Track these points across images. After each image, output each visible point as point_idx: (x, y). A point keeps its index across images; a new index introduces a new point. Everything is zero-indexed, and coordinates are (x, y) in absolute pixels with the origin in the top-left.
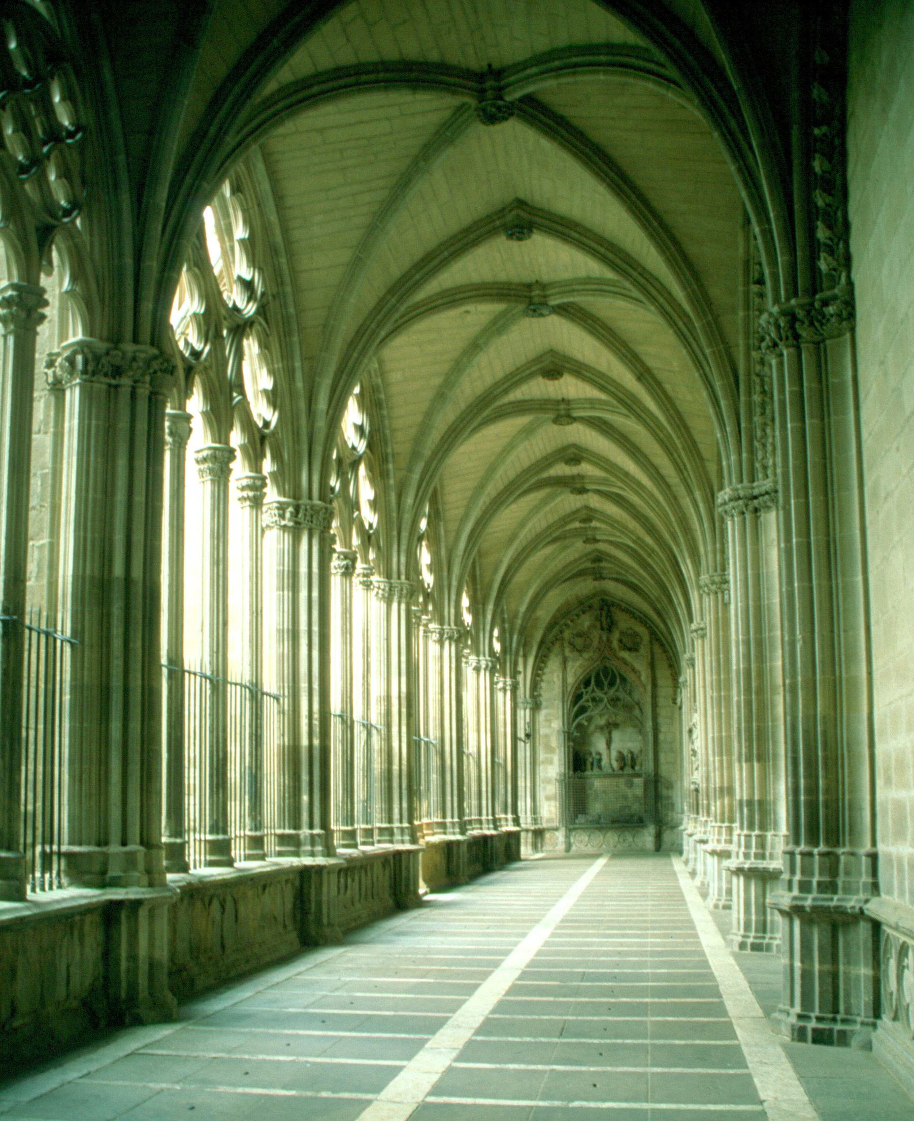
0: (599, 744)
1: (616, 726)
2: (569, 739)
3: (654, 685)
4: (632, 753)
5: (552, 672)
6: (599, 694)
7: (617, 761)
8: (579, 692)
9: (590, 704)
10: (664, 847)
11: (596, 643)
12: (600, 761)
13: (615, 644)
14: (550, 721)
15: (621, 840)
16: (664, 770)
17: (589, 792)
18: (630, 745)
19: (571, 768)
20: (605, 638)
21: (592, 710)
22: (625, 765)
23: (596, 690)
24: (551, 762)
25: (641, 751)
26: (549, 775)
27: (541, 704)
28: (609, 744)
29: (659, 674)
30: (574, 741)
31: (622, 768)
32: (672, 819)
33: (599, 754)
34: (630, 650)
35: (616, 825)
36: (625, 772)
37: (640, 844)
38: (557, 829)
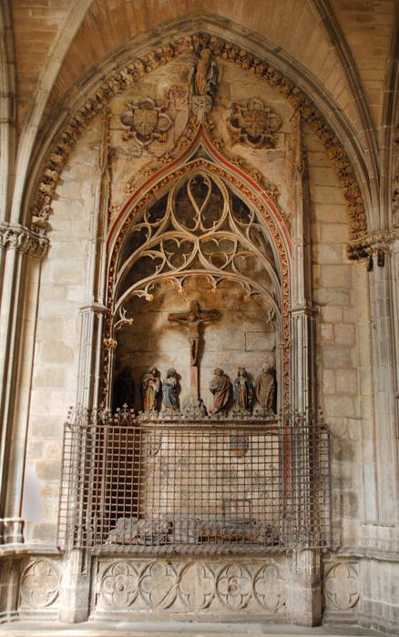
0: (174, 352)
1: (215, 316)
2: (106, 329)
3: (309, 219)
4: (246, 375)
5: (79, 180)
6: (182, 233)
7: (214, 392)
10: (332, 609)
11: (180, 126)
13: (223, 130)
15: (223, 588)
16: (332, 411)
18: (242, 359)
20: (200, 117)
21: (166, 269)
22: (231, 402)
23: (176, 223)
24: (60, 384)
25: (272, 372)
26: (54, 413)
27: (47, 245)
28: (197, 352)
29: (318, 195)
30: (117, 335)
31: (224, 408)
32: (353, 540)
34: (254, 140)
35: (209, 548)
38: (60, 555)
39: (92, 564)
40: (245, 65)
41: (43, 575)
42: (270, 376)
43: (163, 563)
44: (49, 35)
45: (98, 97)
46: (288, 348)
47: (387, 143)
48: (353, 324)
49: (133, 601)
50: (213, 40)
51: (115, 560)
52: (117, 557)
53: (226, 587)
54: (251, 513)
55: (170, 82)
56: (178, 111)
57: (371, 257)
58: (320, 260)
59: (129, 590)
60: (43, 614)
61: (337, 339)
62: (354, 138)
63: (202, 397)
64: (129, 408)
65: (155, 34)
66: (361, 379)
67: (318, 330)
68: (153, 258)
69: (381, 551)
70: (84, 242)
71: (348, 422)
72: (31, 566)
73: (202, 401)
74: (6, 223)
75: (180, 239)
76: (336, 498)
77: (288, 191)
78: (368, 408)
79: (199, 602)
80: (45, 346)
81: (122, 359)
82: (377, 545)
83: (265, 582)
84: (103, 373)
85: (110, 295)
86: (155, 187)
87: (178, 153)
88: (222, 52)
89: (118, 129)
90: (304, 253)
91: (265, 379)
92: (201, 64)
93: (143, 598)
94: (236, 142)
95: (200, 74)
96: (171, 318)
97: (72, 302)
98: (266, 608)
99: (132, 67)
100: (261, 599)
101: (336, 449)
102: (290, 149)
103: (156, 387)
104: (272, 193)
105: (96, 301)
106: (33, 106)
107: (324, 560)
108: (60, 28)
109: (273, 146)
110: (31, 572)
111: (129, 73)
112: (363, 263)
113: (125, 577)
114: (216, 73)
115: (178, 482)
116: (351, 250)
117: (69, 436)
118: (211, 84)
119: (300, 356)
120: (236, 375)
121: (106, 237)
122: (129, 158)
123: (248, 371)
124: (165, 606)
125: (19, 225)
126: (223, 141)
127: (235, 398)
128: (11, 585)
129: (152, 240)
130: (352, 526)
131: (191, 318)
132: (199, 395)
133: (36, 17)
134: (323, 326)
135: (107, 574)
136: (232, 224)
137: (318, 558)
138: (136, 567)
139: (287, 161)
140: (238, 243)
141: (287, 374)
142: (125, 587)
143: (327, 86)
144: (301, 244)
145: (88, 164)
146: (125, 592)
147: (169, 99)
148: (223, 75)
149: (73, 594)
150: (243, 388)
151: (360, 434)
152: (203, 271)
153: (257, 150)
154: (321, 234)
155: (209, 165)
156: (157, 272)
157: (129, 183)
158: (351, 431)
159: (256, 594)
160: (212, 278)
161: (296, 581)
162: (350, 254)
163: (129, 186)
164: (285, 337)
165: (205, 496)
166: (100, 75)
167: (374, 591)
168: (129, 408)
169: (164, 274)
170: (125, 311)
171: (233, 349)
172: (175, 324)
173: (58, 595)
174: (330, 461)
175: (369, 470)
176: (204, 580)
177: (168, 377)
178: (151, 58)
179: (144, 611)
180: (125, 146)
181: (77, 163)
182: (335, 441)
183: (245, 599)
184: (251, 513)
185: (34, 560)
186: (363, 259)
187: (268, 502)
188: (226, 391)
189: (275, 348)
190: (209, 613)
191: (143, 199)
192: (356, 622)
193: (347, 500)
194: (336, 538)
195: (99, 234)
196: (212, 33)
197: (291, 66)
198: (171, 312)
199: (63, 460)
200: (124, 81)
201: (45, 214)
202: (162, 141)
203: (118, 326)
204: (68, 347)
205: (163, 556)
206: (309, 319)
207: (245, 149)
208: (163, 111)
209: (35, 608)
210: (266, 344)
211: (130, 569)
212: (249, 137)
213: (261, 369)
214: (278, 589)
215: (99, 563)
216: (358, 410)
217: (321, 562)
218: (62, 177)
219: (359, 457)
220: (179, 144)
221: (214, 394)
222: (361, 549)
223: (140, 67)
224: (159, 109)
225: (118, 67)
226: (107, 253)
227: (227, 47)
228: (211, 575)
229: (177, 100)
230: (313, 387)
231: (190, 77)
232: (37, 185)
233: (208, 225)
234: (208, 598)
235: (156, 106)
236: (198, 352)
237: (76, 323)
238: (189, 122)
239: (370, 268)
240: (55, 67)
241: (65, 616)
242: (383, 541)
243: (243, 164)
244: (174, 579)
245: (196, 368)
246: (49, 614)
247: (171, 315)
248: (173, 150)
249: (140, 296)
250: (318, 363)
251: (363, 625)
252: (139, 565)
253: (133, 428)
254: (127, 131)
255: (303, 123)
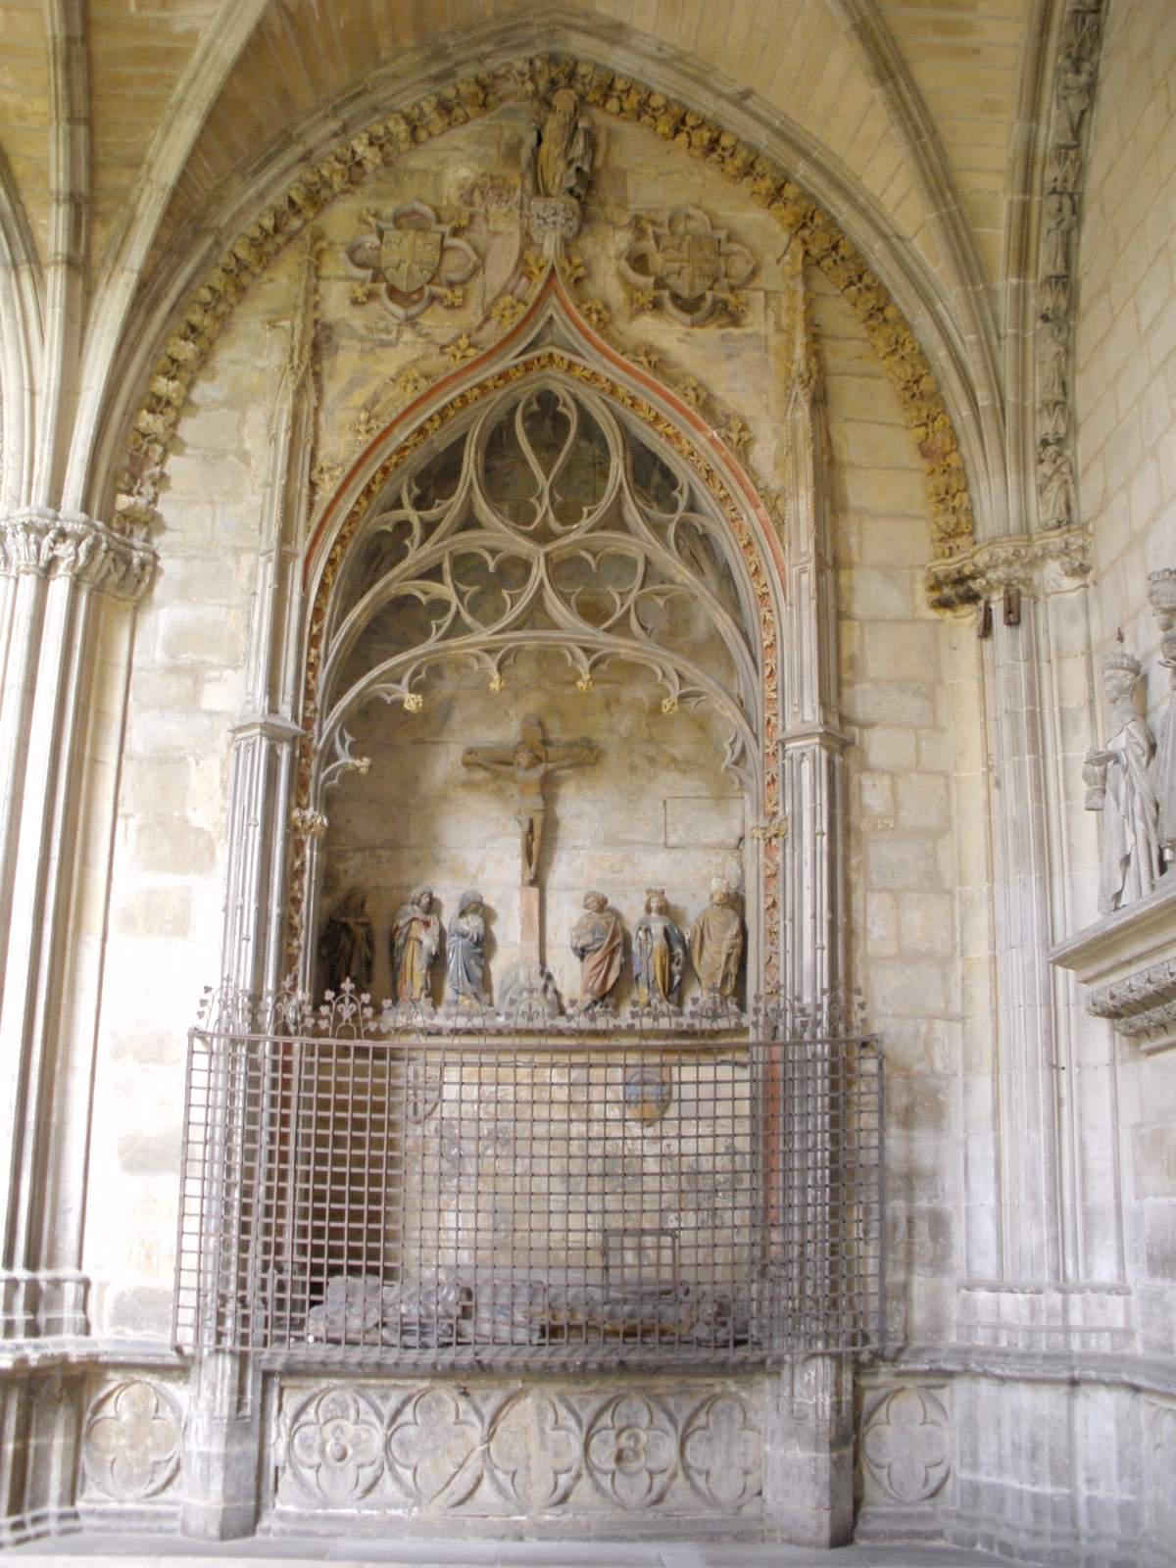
1: (587, 757)
2: (299, 784)
4: (665, 910)
5: (238, 402)
6: (499, 536)
7: (582, 953)
8: (387, 523)
9: (446, 590)
10: (879, 1502)
11: (499, 270)
12: (483, 946)
13: (609, 282)
14: (196, 675)
15: (603, 1456)
17: (411, 1135)
18: (657, 868)
19: (305, 964)
20: (549, 246)
21: (458, 629)
23: (483, 510)
24: (181, 926)
25: (735, 902)
27: (151, 566)
30: (329, 802)
31: (608, 996)
32: (937, 1329)
33: (475, 906)
34: (689, 306)
35: (566, 1352)
36: (625, 1019)
37: (726, 1490)
38: (180, 1368)
39: (265, 1392)
40: (664, 127)
41: (139, 1418)
42: (731, 913)
43: (446, 1392)
44: (173, 55)
45: (291, 202)
46: (777, 836)
47: (1021, 321)
48: (945, 775)
49: (369, 1490)
50: (582, 70)
51: (324, 1383)
52: (329, 1374)
53: (611, 1451)
54: (676, 1265)
55: (475, 166)
56: (495, 234)
57: (987, 603)
58: (858, 609)
59: (360, 1459)
60: (141, 1515)
61: (903, 814)
62: (940, 307)
63: (551, 968)
64: (359, 990)
65: (439, 54)
66: (962, 923)
67: (854, 789)
68: (423, 599)
69: (1007, 1355)
70: (247, 560)
71: (931, 1030)
72: (109, 1395)
73: (549, 977)
74: (51, 512)
75: (493, 552)
76: (895, 1227)
77: (776, 432)
78: (981, 993)
79: (540, 1491)
80: (141, 829)
81: (341, 866)
82: (996, 1340)
83: (709, 1440)
84: (290, 901)
85: (309, 695)
86: (431, 419)
87: (491, 335)
88: (606, 97)
89: (340, 278)
90: (819, 588)
91: (714, 924)
92: (553, 127)
93: (397, 1479)
94: (641, 310)
95: (551, 148)
96: (471, 758)
97: (211, 714)
98: (712, 1502)
99: (380, 130)
100: (700, 1481)
101: (899, 1100)
102: (779, 329)
103: (429, 941)
104: (734, 436)
105: (273, 710)
106: (130, 224)
107: (863, 1382)
108: (204, 38)
109: (735, 321)
110: (109, 1409)
111: (371, 144)
112: (968, 618)
113: (349, 1427)
114: (592, 145)
115: (486, 1186)
116: (936, 585)
117: (201, 1061)
118: (579, 170)
119: (807, 856)
120: (641, 910)
121: (302, 546)
122: (367, 346)
123: (672, 898)
124: (455, 1499)
125: (83, 516)
126: (607, 307)
127: (636, 969)
128: (58, 1442)
129: (422, 553)
130: (936, 1295)
131: (524, 758)
132: (543, 962)
133: (147, 14)
134: (867, 780)
135: (303, 1418)
136: (632, 514)
137: (847, 1377)
138: (378, 1402)
139: (772, 359)
140: (648, 562)
141: (774, 904)
142: (350, 1452)
143: (866, 181)
144: (811, 566)
145: (260, 363)
146: (350, 1464)
147: (472, 204)
148: (608, 150)
149: (217, 1467)
150: (658, 942)
151: (958, 1056)
152: (556, 634)
153: (697, 331)
154: (861, 544)
155: (571, 365)
156: (434, 636)
157: (365, 408)
158: (937, 1050)
159: (686, 1468)
160: (580, 653)
161: (790, 1434)
162: (936, 595)
163: (363, 416)
164: (770, 808)
165: (557, 1222)
166: (298, 150)
167: (986, 1456)
168: (359, 990)
169: (452, 643)
170: (349, 739)
171: (632, 843)
172: (479, 775)
173: (178, 1468)
174: (882, 1128)
175: (981, 1151)
176: (552, 1435)
177: (463, 914)
178: (427, 108)
179: (399, 1512)
180: (357, 320)
181: (234, 362)
182: (896, 1081)
183: (659, 1481)
184: (676, 1265)
185: (115, 1379)
186: (967, 609)
187: (723, 1235)
188: (613, 952)
189: (741, 839)
190: (565, 1518)
191: (401, 450)
192: (939, 1534)
193: (923, 1228)
194: (895, 1325)
195: (285, 537)
196: (581, 55)
197: (780, 134)
198: (471, 745)
199: (188, 1123)
200: (359, 164)
201: (148, 490)
202: (452, 307)
203: (330, 777)
204: (200, 831)
205: (451, 1372)
206: (830, 762)
207: (665, 326)
208: (456, 232)
209: (121, 1501)
210: (720, 830)
211: (363, 1404)
212: (676, 298)
213: (707, 896)
214: (745, 1455)
215: (281, 1390)
216: (956, 997)
217: (855, 1385)
218: (196, 396)
219: (955, 1117)
220: (495, 312)
221: (582, 958)
222: (955, 1351)
223: (401, 129)
224: (447, 229)
225: (345, 129)
226: (305, 585)
227: (620, 85)
228: (572, 1423)
229: (493, 208)
230: (840, 936)
231: (525, 154)
232: (131, 416)
233: (567, 515)
234: (563, 1479)
235: (439, 221)
236: (541, 851)
237: (223, 768)
238: (522, 260)
239: (986, 630)
240: (188, 127)
241: (195, 1524)
242: (1011, 1328)
243: (658, 363)
244: (476, 1432)
245: (535, 891)
246: (157, 1516)
247: (470, 752)
248: (480, 328)
249: (389, 699)
250: (854, 877)
251: (957, 1540)
252: (385, 1397)
253: (369, 1043)
254: (363, 282)
255: (810, 264)
